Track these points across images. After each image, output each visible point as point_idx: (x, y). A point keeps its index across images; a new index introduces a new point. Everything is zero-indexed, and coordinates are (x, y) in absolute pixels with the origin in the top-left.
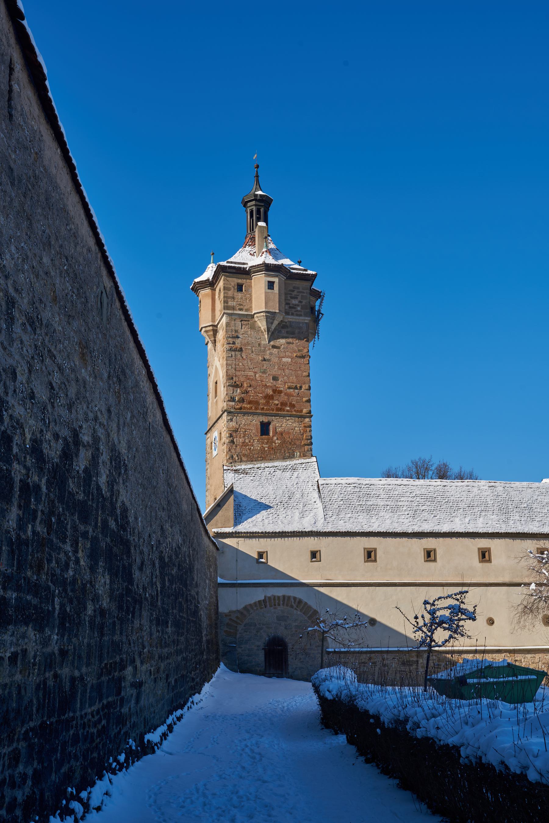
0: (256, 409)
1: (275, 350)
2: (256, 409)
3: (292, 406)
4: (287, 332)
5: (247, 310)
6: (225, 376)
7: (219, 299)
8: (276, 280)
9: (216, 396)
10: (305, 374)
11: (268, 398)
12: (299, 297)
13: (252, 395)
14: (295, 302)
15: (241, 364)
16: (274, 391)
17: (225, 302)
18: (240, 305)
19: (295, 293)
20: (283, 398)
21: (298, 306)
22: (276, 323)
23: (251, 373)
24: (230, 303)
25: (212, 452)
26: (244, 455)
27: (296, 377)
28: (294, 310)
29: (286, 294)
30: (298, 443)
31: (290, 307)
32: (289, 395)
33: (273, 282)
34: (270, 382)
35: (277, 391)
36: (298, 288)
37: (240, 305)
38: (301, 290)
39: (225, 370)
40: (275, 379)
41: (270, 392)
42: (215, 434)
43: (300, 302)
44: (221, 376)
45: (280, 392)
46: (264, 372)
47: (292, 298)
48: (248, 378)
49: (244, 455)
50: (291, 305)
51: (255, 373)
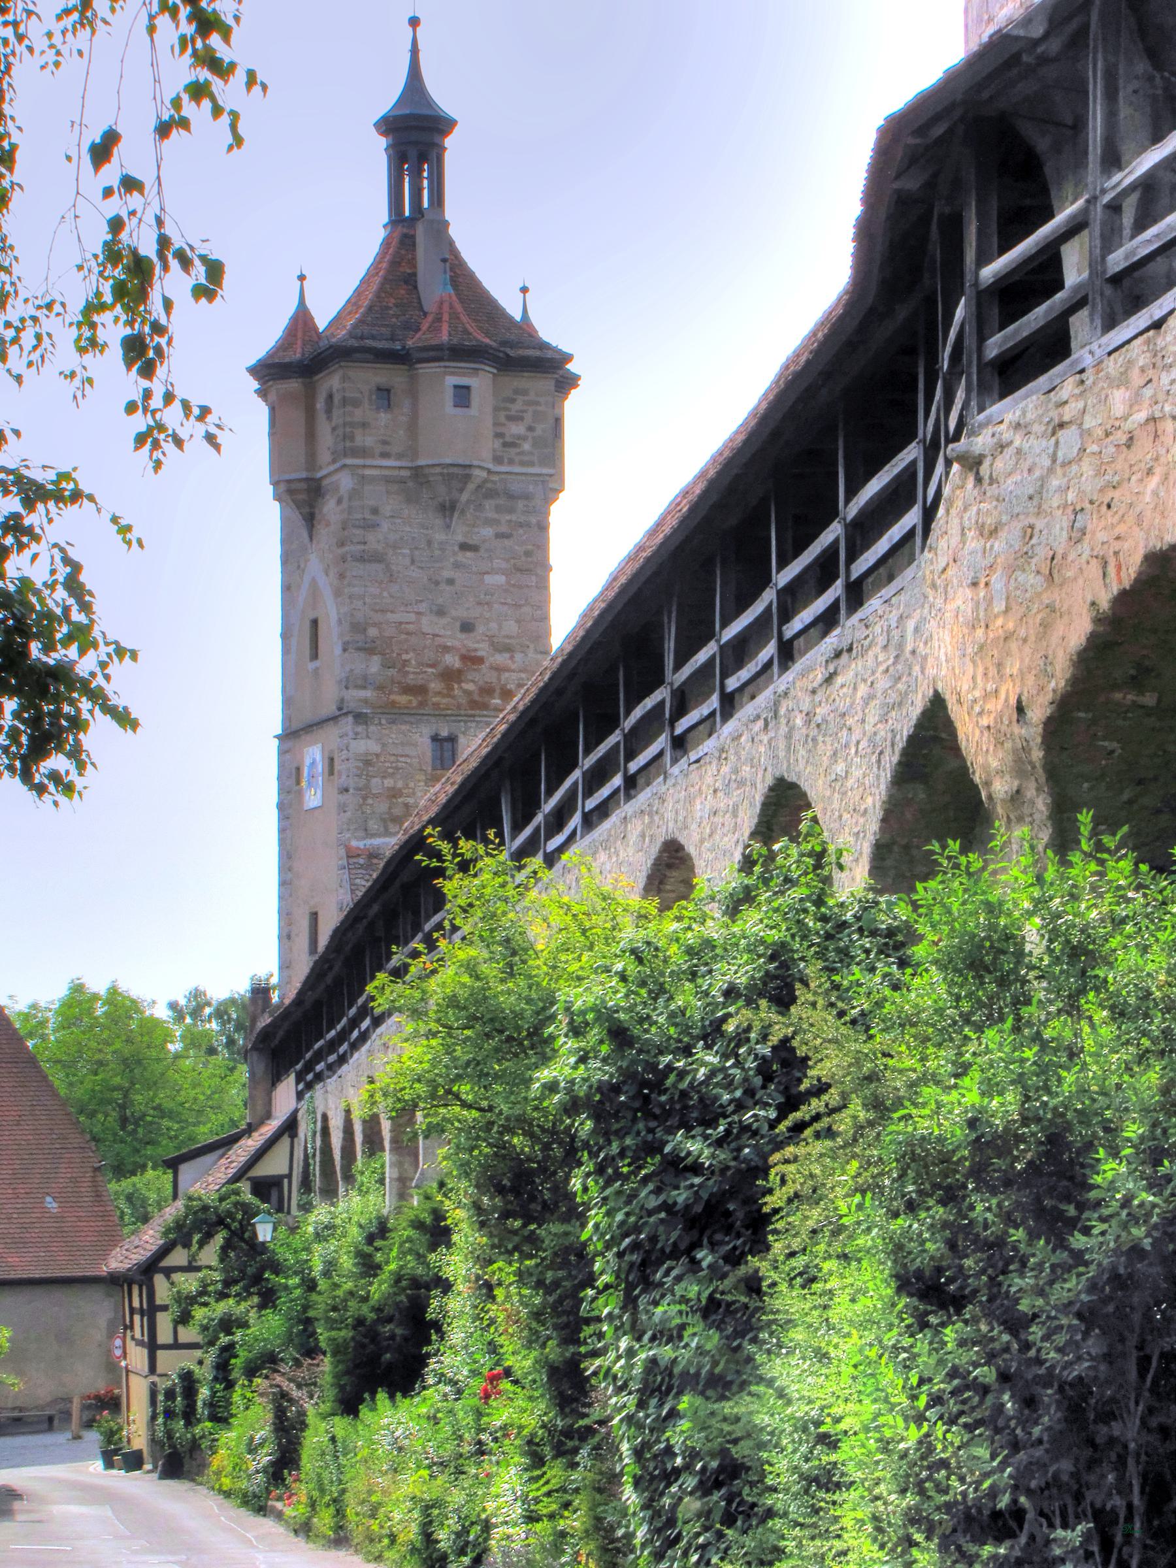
1: (469, 554)
5: (399, 456)
9: (315, 655)
11: (450, 676)
12: (528, 417)
14: (517, 429)
15: (385, 594)
16: (464, 658)
18: (385, 443)
20: (485, 675)
21: (525, 438)
23: (412, 617)
27: (518, 621)
28: (513, 451)
29: (496, 409)
31: (505, 445)
33: (468, 388)
35: (472, 660)
37: (385, 443)
38: (532, 396)
41: (452, 661)
43: (531, 429)
44: (333, 615)
45: (480, 660)
46: (441, 613)
47: (510, 418)
50: (508, 439)
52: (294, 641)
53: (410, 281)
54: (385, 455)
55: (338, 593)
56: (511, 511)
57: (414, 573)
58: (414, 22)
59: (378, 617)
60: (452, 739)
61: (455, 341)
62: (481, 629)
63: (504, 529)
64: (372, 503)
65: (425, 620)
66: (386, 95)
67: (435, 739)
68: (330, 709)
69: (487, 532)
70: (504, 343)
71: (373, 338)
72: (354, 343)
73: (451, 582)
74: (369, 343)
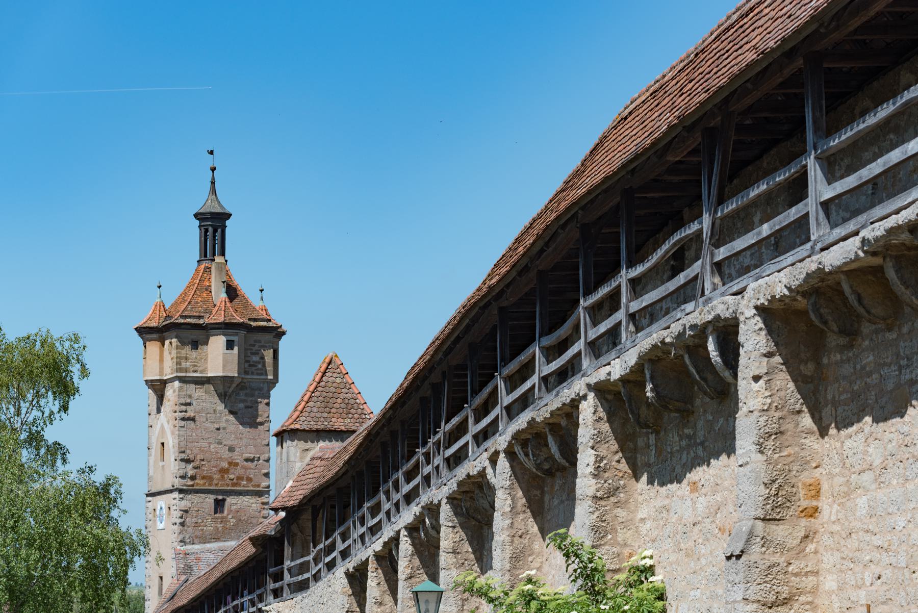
0: (210, 485)
2: (210, 485)
3: (249, 480)
4: (246, 395)
5: (202, 372)
6: (176, 449)
7: (170, 353)
8: (235, 338)
10: (265, 442)
11: (223, 471)
13: (205, 470)
16: (230, 464)
17: (178, 363)
19: (256, 348)
20: (239, 471)
21: (259, 363)
22: (234, 385)
23: (205, 445)
24: (184, 364)
25: (155, 521)
26: (196, 537)
28: (254, 368)
29: (246, 349)
30: (254, 521)
31: (250, 366)
32: (246, 468)
34: (226, 454)
36: (260, 342)
39: (176, 441)
40: (231, 449)
41: (225, 465)
42: (161, 502)
45: (237, 464)
47: (252, 354)
48: (201, 450)
49: (196, 537)
51: (210, 443)
52: (153, 451)
53: (208, 289)
54: (195, 371)
55: (173, 433)
56: (253, 395)
57: (208, 425)
58: (213, 169)
59: (190, 445)
60: (224, 500)
61: (227, 321)
62: (237, 450)
63: (249, 404)
64: (188, 393)
65: (212, 446)
66: (200, 201)
67: (216, 501)
68: (168, 486)
69: (241, 405)
70: (250, 319)
71: (190, 317)
72: (181, 320)
73: (224, 428)
74: (188, 320)
